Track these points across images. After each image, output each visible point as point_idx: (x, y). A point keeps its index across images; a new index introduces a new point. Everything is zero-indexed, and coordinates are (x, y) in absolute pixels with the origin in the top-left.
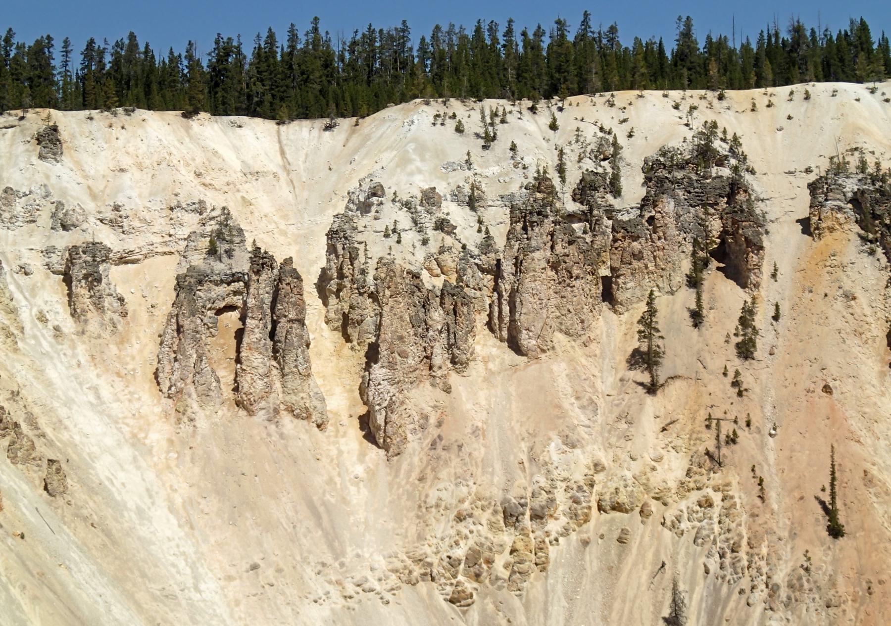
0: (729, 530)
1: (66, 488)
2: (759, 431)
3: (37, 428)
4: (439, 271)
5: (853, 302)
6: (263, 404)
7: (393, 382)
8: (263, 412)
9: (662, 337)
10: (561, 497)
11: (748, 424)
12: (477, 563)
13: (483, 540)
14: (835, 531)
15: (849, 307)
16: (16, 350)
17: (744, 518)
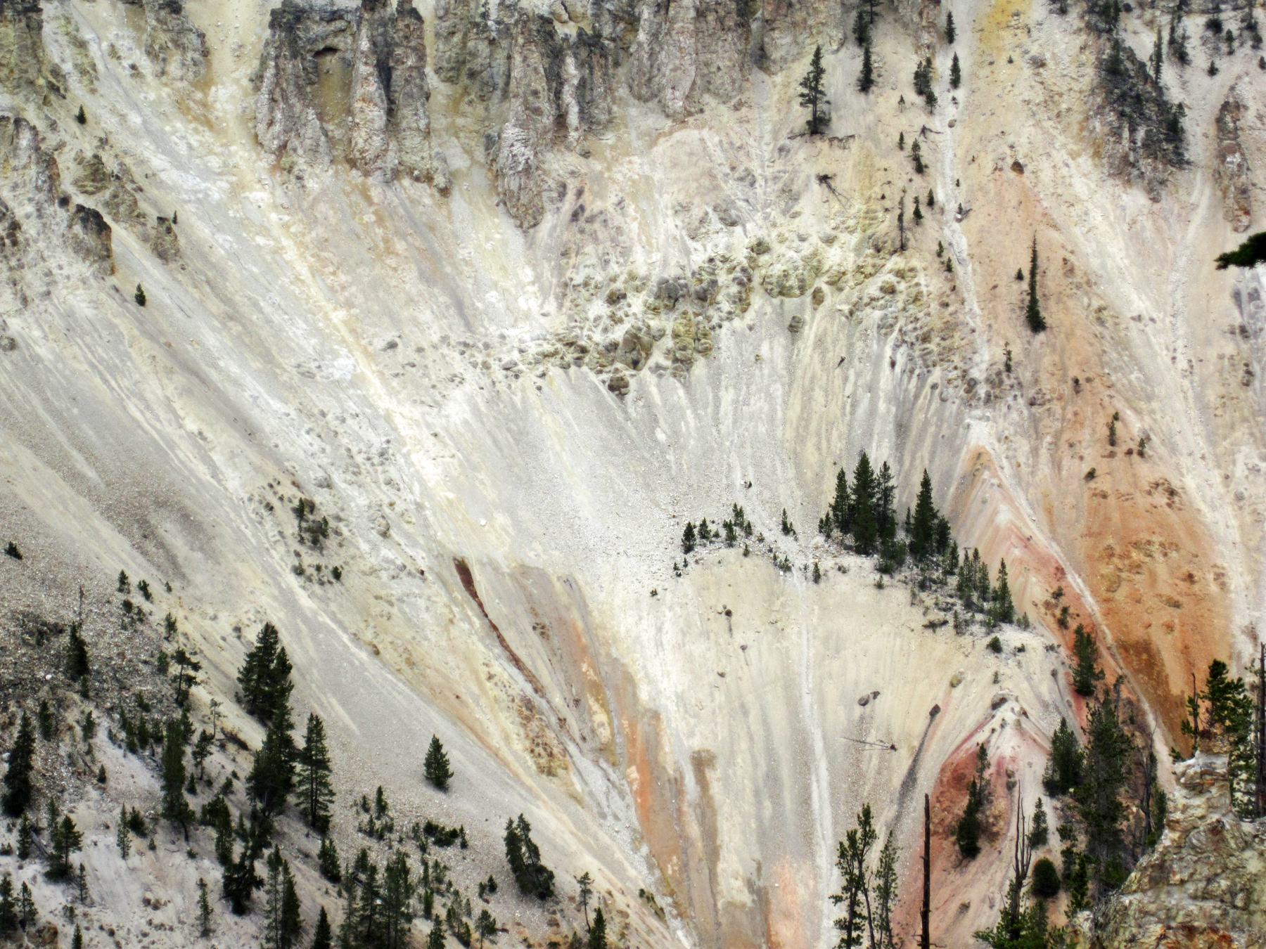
0: (917, 320)
1: (178, 251)
2: (942, 211)
3: (133, 182)
4: (565, 17)
5: (1041, 70)
6: (379, 163)
7: (525, 143)
8: (378, 173)
9: (828, 102)
10: (723, 278)
11: (931, 202)
12: (636, 349)
13: (640, 324)
14: (1036, 323)
15: (1038, 74)
16: (93, 91)
17: (934, 306)
